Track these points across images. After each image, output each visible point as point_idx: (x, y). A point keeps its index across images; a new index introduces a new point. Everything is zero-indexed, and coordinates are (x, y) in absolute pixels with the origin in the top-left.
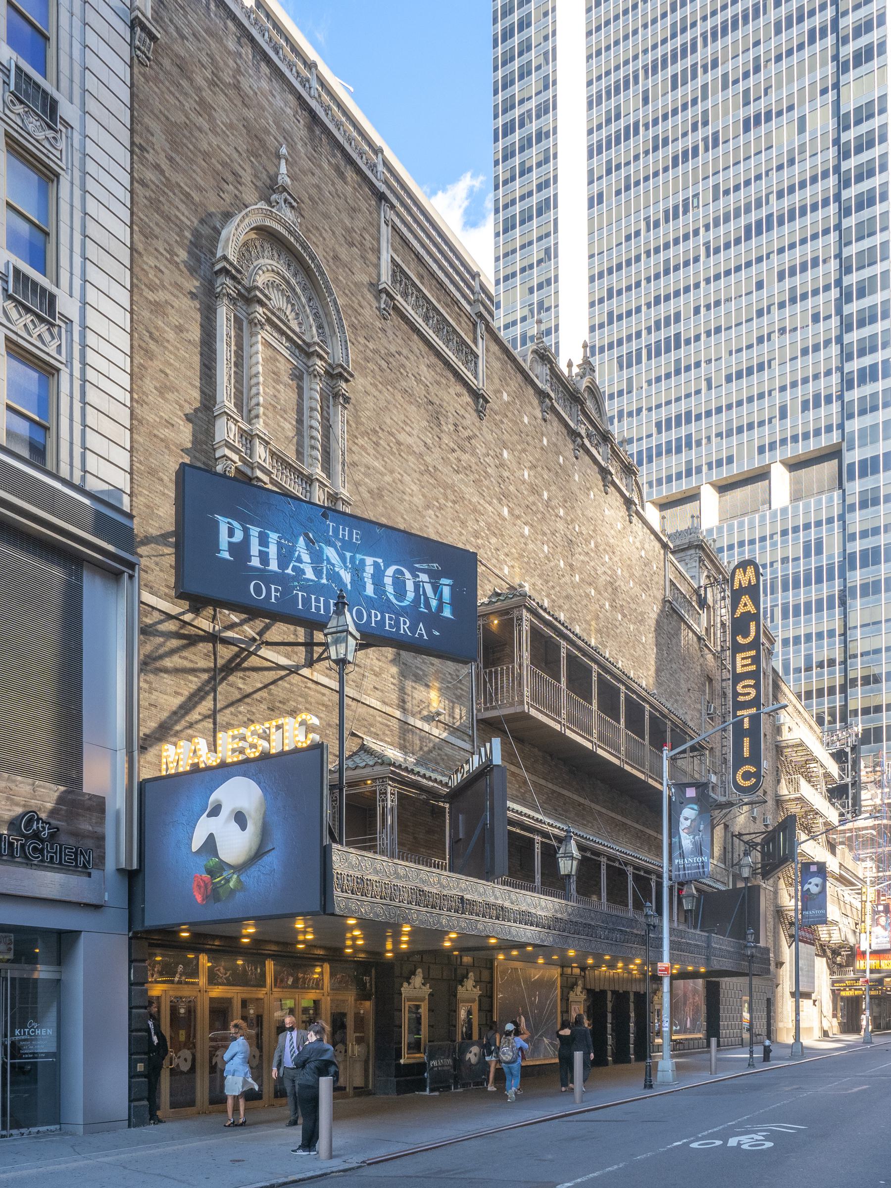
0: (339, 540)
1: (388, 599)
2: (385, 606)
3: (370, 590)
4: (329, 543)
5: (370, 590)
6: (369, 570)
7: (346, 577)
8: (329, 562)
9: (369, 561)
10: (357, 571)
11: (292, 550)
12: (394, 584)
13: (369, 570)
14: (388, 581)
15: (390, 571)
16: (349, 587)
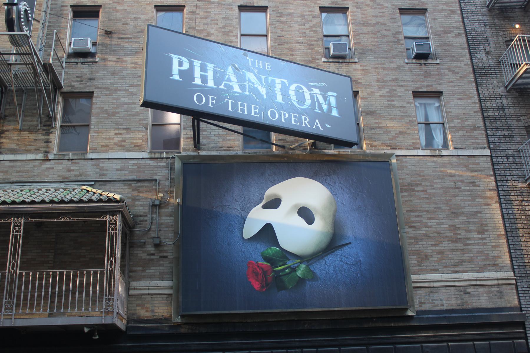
0: (257, 68)
1: (293, 105)
2: (292, 109)
3: (279, 99)
4: (249, 70)
5: (279, 99)
6: (278, 86)
7: (263, 91)
8: (250, 81)
9: (278, 81)
10: (270, 87)
11: (223, 74)
12: (296, 95)
13: (278, 86)
14: (292, 93)
15: (293, 87)
16: (265, 96)
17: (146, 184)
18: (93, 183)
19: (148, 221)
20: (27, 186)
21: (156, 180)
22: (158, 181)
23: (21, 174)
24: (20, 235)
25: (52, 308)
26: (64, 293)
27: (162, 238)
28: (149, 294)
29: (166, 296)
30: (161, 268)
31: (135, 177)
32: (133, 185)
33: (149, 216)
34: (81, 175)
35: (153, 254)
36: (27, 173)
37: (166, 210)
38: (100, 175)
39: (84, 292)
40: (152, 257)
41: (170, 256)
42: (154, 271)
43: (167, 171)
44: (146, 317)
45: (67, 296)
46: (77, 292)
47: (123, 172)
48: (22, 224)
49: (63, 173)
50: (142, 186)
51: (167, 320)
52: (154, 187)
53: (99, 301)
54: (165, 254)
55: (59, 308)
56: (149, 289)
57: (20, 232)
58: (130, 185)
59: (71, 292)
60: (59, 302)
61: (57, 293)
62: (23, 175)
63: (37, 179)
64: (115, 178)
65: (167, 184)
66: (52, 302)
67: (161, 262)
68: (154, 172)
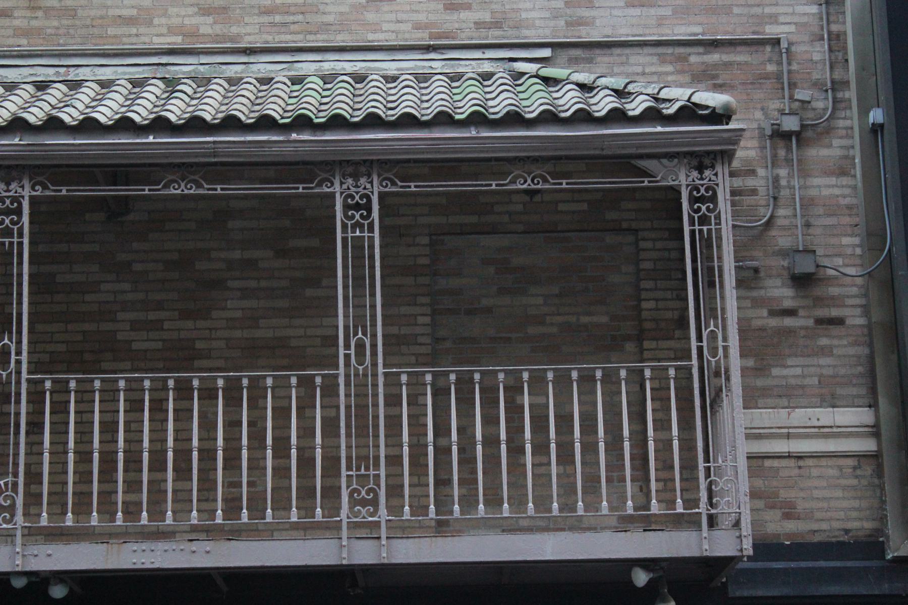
17: (741, 56)
18: (546, 53)
19: (762, 191)
20: (307, 66)
21: (777, 42)
22: (784, 45)
23: (278, 18)
24: (371, 239)
25: (443, 504)
26: (479, 448)
27: (820, 252)
28: (789, 456)
29: (850, 462)
30: (824, 361)
31: (698, 29)
32: (693, 59)
33: (761, 172)
34: (497, 25)
35: (791, 312)
36: (300, 18)
37: (824, 152)
38: (568, 24)
39: (553, 446)
40: (788, 322)
41: (856, 319)
42: (798, 371)
43: (814, 9)
44: (788, 536)
45: (492, 461)
46: (528, 447)
47: (653, 11)
48: (375, 199)
49: (432, 17)
50: (728, 65)
51: (872, 546)
52: (771, 68)
53: (609, 480)
54: (835, 313)
55: (469, 502)
56: (788, 436)
57: (371, 228)
58: (683, 59)
59: (503, 447)
60: (468, 481)
61: (455, 448)
62: (285, 24)
63: (340, 40)
64: (624, 33)
65: (816, 57)
66: (443, 482)
67: (824, 341)
68: (767, 10)
